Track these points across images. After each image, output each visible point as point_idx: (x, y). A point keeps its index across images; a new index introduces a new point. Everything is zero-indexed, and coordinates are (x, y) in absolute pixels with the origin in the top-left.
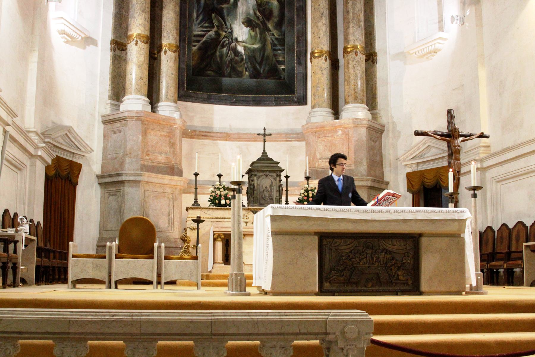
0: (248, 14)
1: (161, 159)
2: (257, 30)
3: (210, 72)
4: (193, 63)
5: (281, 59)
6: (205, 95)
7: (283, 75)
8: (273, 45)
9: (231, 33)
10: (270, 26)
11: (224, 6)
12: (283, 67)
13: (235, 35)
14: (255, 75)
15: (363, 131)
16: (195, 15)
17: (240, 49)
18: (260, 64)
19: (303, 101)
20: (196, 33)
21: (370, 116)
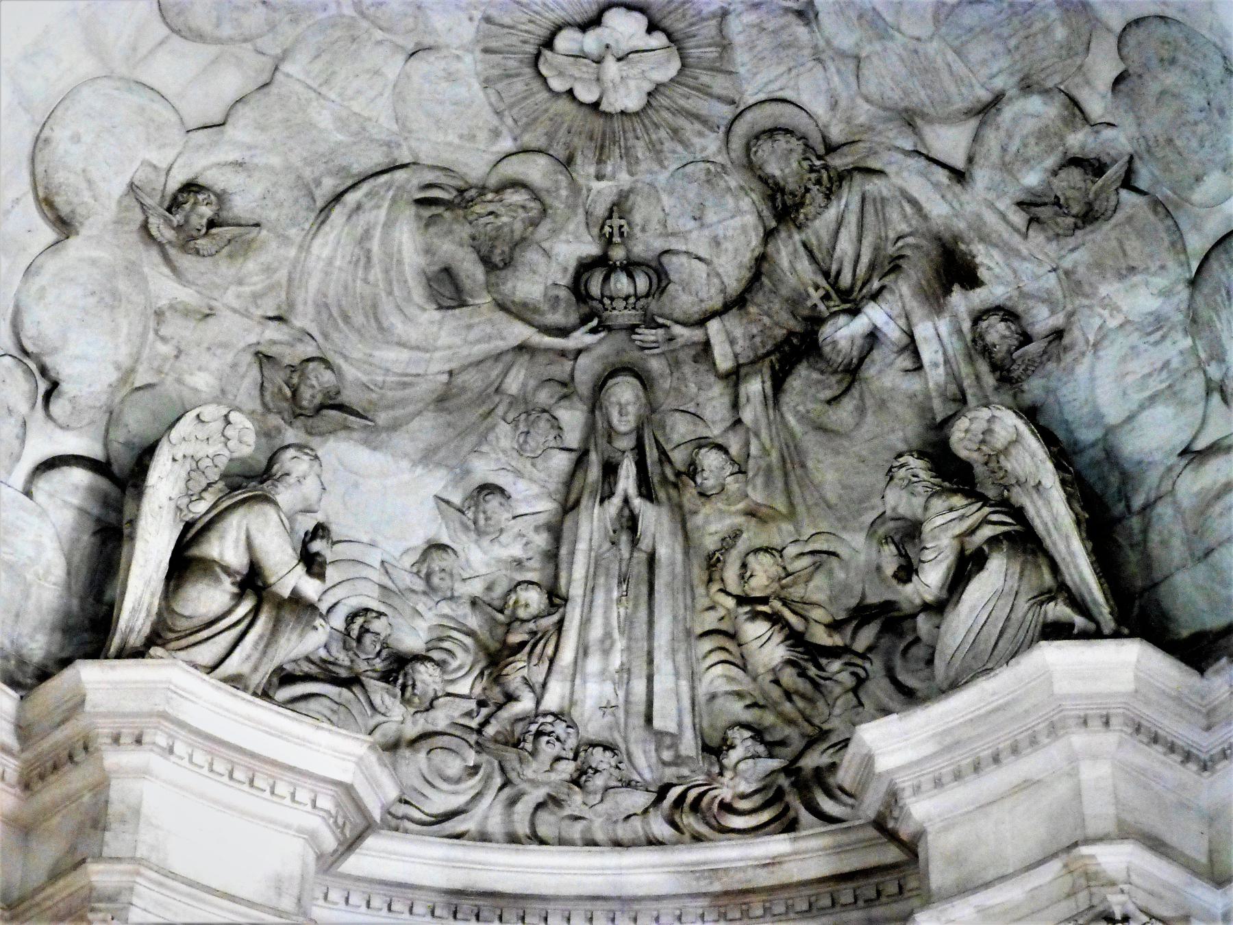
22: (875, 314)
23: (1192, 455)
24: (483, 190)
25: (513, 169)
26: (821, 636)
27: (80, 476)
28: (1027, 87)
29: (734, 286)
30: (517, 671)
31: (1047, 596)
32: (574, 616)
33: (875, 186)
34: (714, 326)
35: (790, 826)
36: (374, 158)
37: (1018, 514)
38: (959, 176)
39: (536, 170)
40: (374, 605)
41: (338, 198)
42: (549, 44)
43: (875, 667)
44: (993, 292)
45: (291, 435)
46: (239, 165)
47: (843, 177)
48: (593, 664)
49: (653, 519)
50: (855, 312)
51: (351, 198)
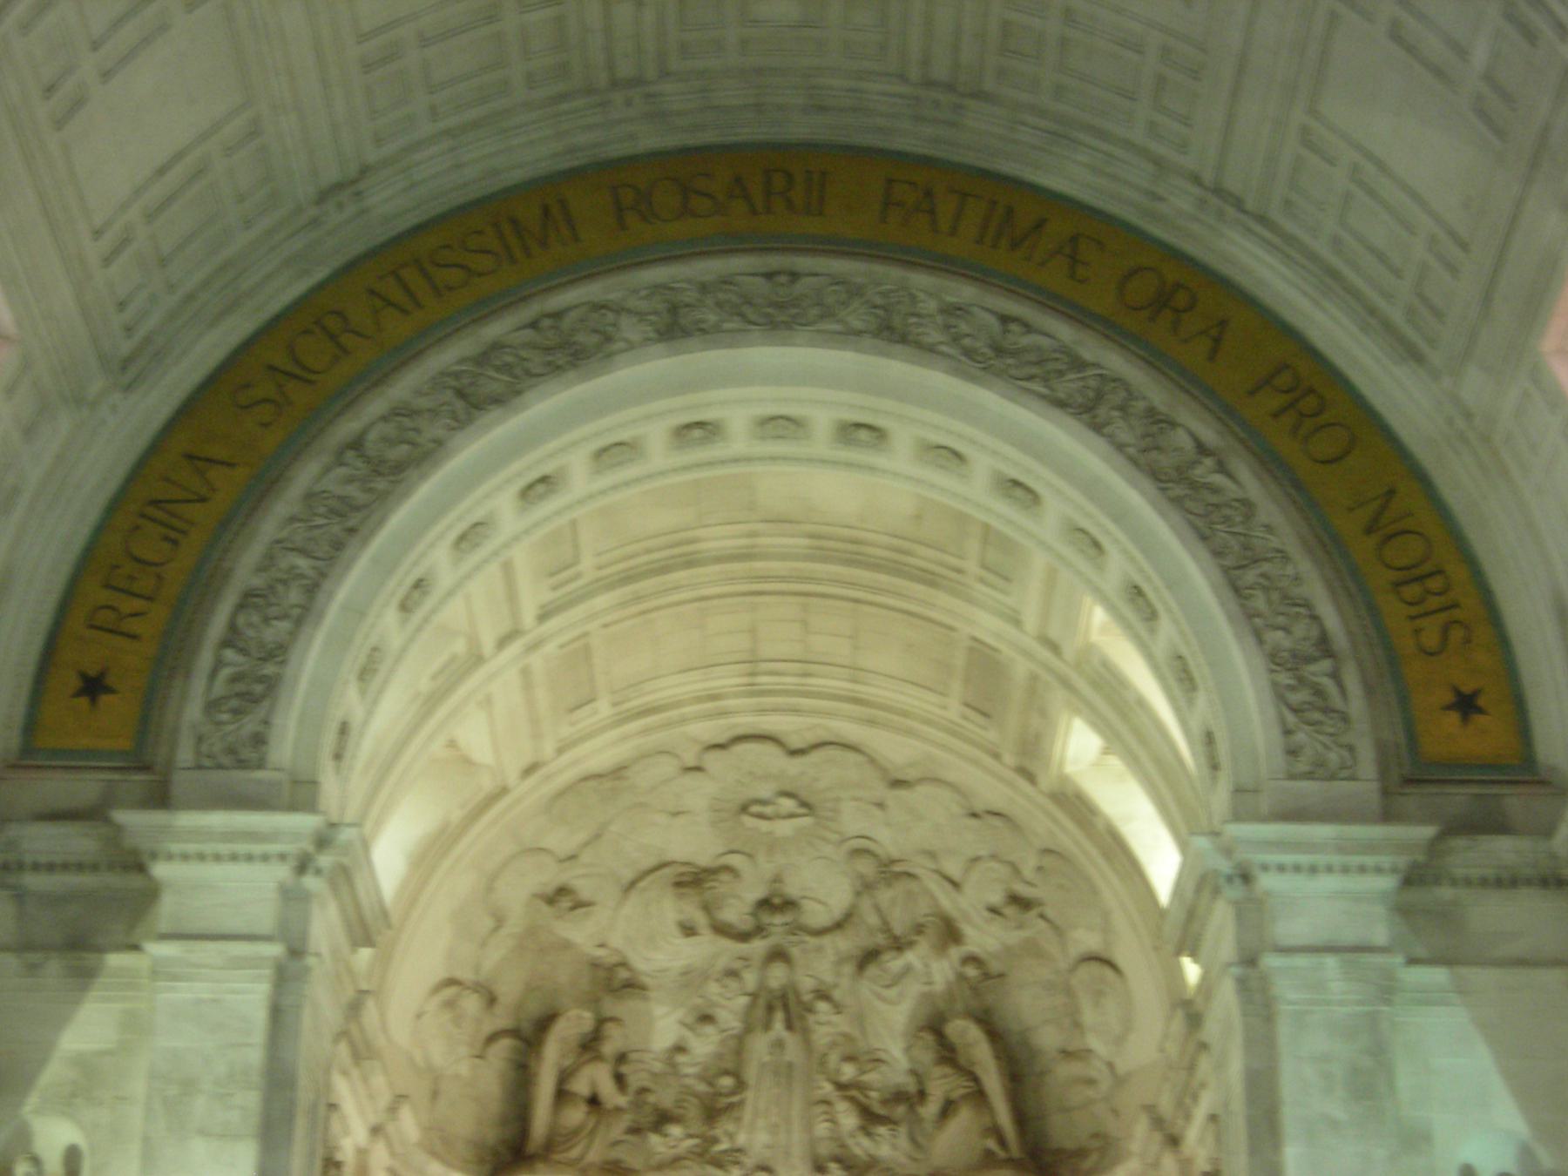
22: (910, 957)
23: (1067, 1054)
24: (712, 872)
28: (994, 857)
30: (724, 1126)
32: (749, 1095)
33: (913, 886)
34: (826, 940)
36: (651, 861)
37: (976, 1079)
38: (955, 884)
39: (735, 860)
40: (646, 1084)
41: (633, 884)
43: (903, 1130)
45: (611, 1007)
46: (584, 876)
48: (761, 1123)
51: (642, 884)
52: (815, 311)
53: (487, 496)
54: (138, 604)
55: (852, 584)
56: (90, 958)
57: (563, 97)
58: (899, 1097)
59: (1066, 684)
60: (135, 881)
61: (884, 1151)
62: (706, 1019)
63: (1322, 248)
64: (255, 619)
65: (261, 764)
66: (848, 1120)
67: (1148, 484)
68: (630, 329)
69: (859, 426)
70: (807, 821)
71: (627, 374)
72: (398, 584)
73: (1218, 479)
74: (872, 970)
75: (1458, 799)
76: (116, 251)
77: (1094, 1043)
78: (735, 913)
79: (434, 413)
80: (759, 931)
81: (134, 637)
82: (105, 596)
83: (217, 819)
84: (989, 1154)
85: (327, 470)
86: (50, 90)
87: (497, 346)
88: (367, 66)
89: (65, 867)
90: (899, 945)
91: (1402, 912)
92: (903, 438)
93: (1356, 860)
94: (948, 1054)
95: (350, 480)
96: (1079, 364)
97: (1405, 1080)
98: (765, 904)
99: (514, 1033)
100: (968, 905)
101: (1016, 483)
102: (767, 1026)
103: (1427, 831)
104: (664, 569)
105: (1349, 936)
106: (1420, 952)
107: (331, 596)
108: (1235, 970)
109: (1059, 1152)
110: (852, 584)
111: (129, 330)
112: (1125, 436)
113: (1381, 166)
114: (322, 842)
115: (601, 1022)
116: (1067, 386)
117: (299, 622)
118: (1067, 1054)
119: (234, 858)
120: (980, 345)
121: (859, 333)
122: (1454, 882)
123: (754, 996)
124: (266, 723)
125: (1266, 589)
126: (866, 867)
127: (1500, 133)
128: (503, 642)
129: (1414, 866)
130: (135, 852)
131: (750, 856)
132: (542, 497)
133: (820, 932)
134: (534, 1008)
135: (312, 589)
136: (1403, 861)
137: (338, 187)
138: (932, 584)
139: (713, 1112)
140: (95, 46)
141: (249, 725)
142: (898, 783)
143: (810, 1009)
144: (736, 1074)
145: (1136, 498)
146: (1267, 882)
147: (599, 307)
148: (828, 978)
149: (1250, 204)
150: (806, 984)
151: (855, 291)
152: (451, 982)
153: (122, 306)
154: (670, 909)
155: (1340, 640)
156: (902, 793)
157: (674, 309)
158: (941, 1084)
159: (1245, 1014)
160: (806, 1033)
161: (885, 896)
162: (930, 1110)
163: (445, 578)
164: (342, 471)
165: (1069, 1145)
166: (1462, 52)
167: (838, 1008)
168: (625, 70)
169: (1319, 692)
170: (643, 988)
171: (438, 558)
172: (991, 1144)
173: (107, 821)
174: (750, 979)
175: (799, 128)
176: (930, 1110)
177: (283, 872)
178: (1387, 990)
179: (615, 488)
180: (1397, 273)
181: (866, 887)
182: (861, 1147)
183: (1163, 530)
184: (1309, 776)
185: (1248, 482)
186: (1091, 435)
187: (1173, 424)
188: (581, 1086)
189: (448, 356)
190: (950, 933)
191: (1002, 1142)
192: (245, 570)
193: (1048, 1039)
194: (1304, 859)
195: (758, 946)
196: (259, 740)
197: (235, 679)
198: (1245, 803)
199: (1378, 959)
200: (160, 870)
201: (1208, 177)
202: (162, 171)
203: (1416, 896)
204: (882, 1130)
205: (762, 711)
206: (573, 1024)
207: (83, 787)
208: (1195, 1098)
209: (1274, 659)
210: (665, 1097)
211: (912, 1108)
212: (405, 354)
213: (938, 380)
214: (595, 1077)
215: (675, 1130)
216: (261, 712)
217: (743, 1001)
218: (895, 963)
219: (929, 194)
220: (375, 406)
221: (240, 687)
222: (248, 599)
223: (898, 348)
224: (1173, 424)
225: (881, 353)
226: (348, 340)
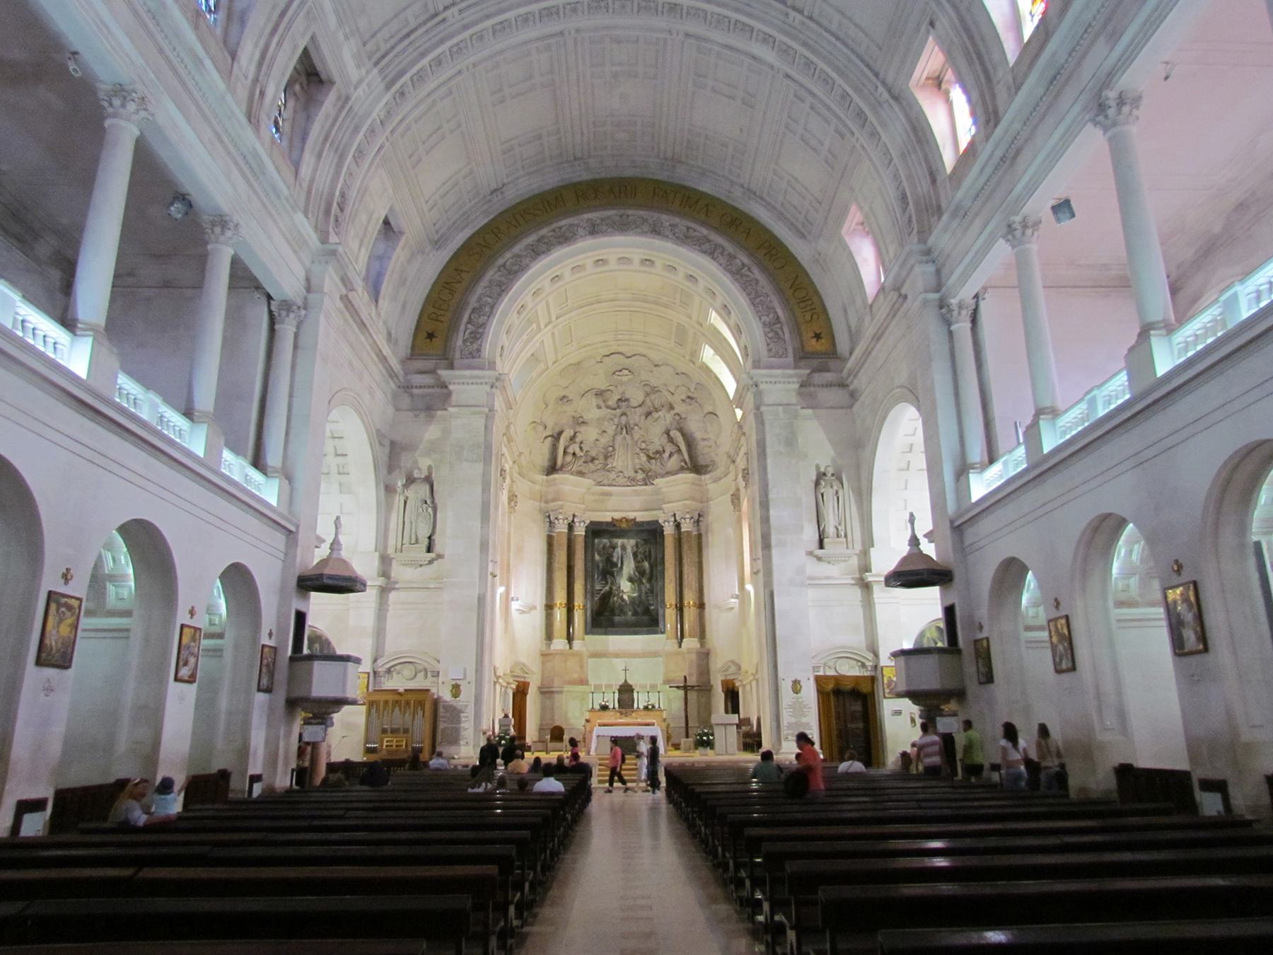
0: (630, 574)
1: (576, 676)
2: (636, 584)
3: (606, 614)
4: (596, 608)
5: (651, 602)
6: (603, 630)
7: (654, 613)
8: (646, 593)
9: (619, 587)
10: (644, 581)
11: (615, 569)
12: (652, 608)
13: (622, 588)
14: (635, 613)
15: (694, 656)
16: (596, 576)
17: (625, 597)
18: (638, 606)
19: (662, 633)
20: (598, 588)
21: (698, 646)
22: (660, 413)
25: (610, 388)
26: (651, 455)
27: (550, 438)
28: (683, 386)
29: (640, 402)
30: (610, 460)
31: (681, 461)
32: (617, 452)
35: (646, 484)
39: (610, 388)
42: (614, 373)
44: (676, 411)
47: (657, 391)
49: (628, 437)
50: (657, 412)
52: (634, 226)
53: (541, 281)
54: (442, 312)
55: (644, 308)
56: (433, 412)
57: (562, 163)
58: (657, 452)
59: (703, 334)
60: (445, 391)
61: (653, 467)
62: (604, 432)
63: (778, 206)
64: (476, 316)
65: (479, 357)
66: (644, 458)
67: (728, 275)
68: (581, 232)
69: (646, 260)
70: (632, 376)
71: (580, 244)
72: (517, 306)
73: (748, 273)
74: (649, 417)
75: (815, 362)
76: (432, 208)
77: (711, 436)
78: (612, 403)
79: (526, 256)
80: (619, 407)
81: (442, 322)
82: (433, 310)
83: (468, 373)
84: (682, 467)
85: (496, 272)
86: (411, 156)
87: (543, 237)
88: (504, 153)
89: (425, 387)
90: (657, 410)
91: (800, 394)
92: (659, 264)
93: (787, 380)
94: (671, 440)
95: (502, 276)
96: (709, 241)
97: (800, 440)
98: (620, 400)
99: (552, 436)
100: (676, 400)
101: (691, 276)
102: (621, 434)
103: (808, 371)
104: (592, 304)
105: (786, 401)
106: (805, 406)
107: (498, 309)
108: (754, 411)
109: (701, 466)
110: (644, 308)
111: (437, 232)
112: (722, 261)
113: (796, 179)
114: (497, 379)
115: (575, 433)
116: (706, 246)
117: (489, 317)
118: (704, 440)
119: (472, 383)
120: (681, 235)
121: (646, 232)
122: (814, 386)
123: (618, 426)
124: (481, 345)
125: (762, 305)
126: (648, 389)
127: (832, 168)
128: (546, 326)
129: (803, 381)
130: (444, 382)
131: (616, 387)
132: (557, 281)
133: (635, 408)
134: (557, 430)
135: (493, 307)
136: (800, 380)
137: (496, 190)
138: (667, 307)
139: (606, 457)
140: (424, 143)
141: (475, 346)
142: (656, 366)
143: (633, 429)
144: (613, 447)
145: (726, 279)
146: (762, 387)
147: (571, 225)
148: (637, 418)
149: (758, 194)
150: (632, 422)
151: (645, 221)
152: (535, 422)
153: (434, 225)
154: (594, 401)
155: (782, 318)
156: (657, 368)
157: (594, 226)
158: (669, 448)
159: (756, 422)
160: (632, 436)
161: (653, 397)
162: (666, 455)
163: (530, 305)
164: (499, 273)
165: (704, 464)
166: (822, 144)
167: (640, 429)
168: (579, 155)
169: (776, 333)
170: (586, 423)
171: (527, 298)
172: (683, 464)
173: (437, 374)
174: (616, 420)
175: (629, 173)
176: (666, 455)
177: (488, 388)
178: (796, 416)
179: (577, 279)
180: (800, 213)
181: (648, 395)
182: (647, 466)
183: (734, 288)
184: (774, 357)
185: (757, 273)
186: (712, 260)
187: (736, 258)
188: (570, 450)
189: (531, 239)
190: (672, 408)
191: (686, 464)
192: (473, 302)
193: (698, 435)
194: (773, 380)
195: (618, 412)
196: (479, 350)
197: (471, 333)
198: (757, 364)
199: (793, 407)
200: (451, 387)
201: (746, 186)
202: (444, 184)
203: (803, 389)
204: (653, 461)
205: (619, 345)
206: (568, 433)
207: (429, 364)
208: (740, 449)
209: (764, 324)
210: (593, 454)
211: (661, 455)
212: (516, 239)
213: (669, 245)
214: (574, 448)
215: (596, 462)
216: (479, 342)
217: (615, 427)
218: (655, 415)
219: (666, 192)
220: (508, 255)
221: (473, 335)
222: (474, 310)
223: (658, 237)
224: (736, 258)
225: (653, 238)
226: (500, 235)
